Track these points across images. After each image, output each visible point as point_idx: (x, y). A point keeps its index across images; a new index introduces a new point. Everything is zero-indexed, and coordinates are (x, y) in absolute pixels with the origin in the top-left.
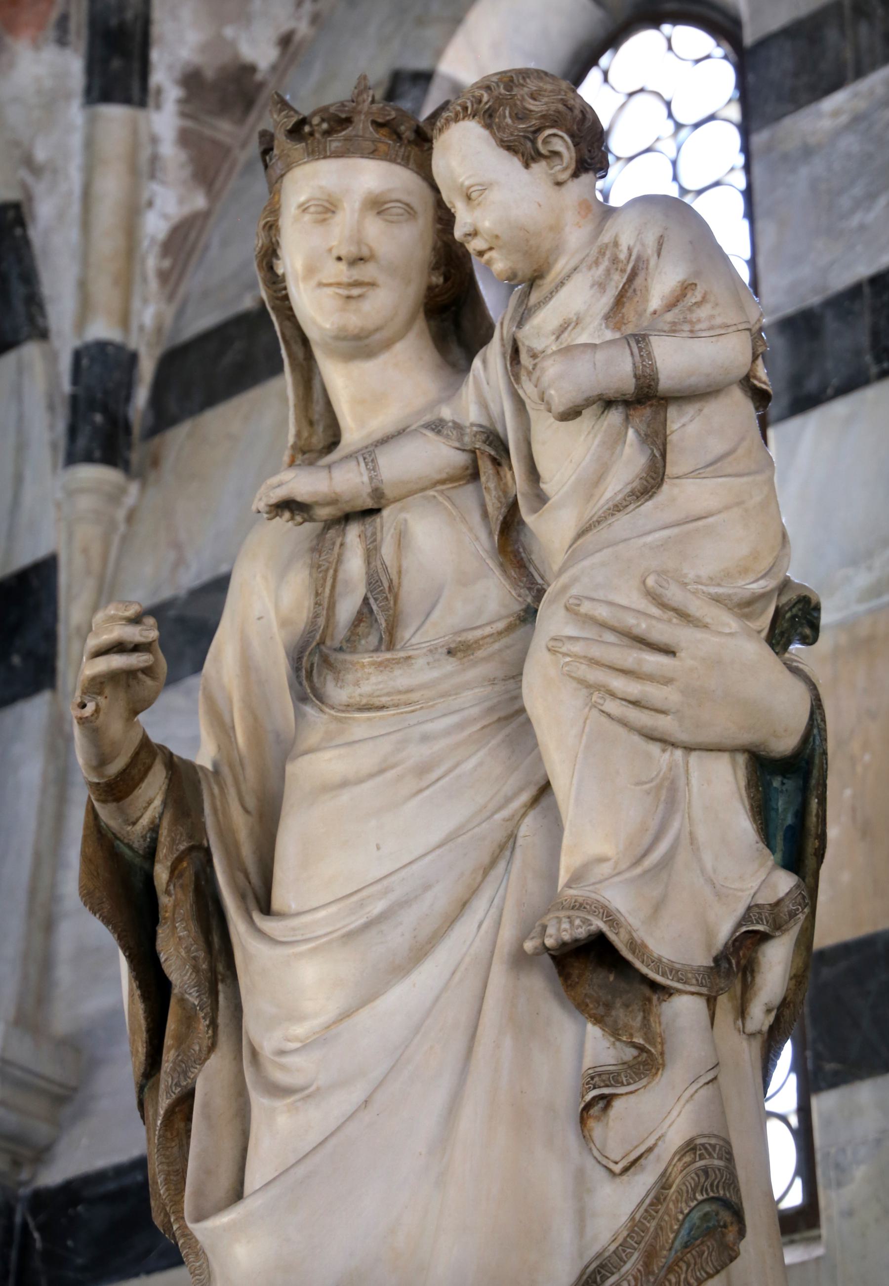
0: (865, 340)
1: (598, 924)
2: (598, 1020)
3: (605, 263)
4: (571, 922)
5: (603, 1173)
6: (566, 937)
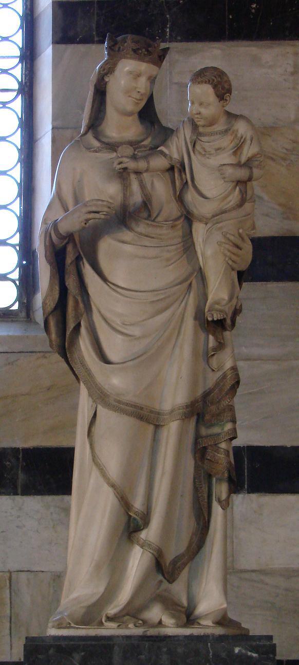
0: (94, 26)
1: (225, 316)
2: (213, 335)
3: (234, 135)
4: (220, 315)
5: (210, 370)
6: (219, 319)
